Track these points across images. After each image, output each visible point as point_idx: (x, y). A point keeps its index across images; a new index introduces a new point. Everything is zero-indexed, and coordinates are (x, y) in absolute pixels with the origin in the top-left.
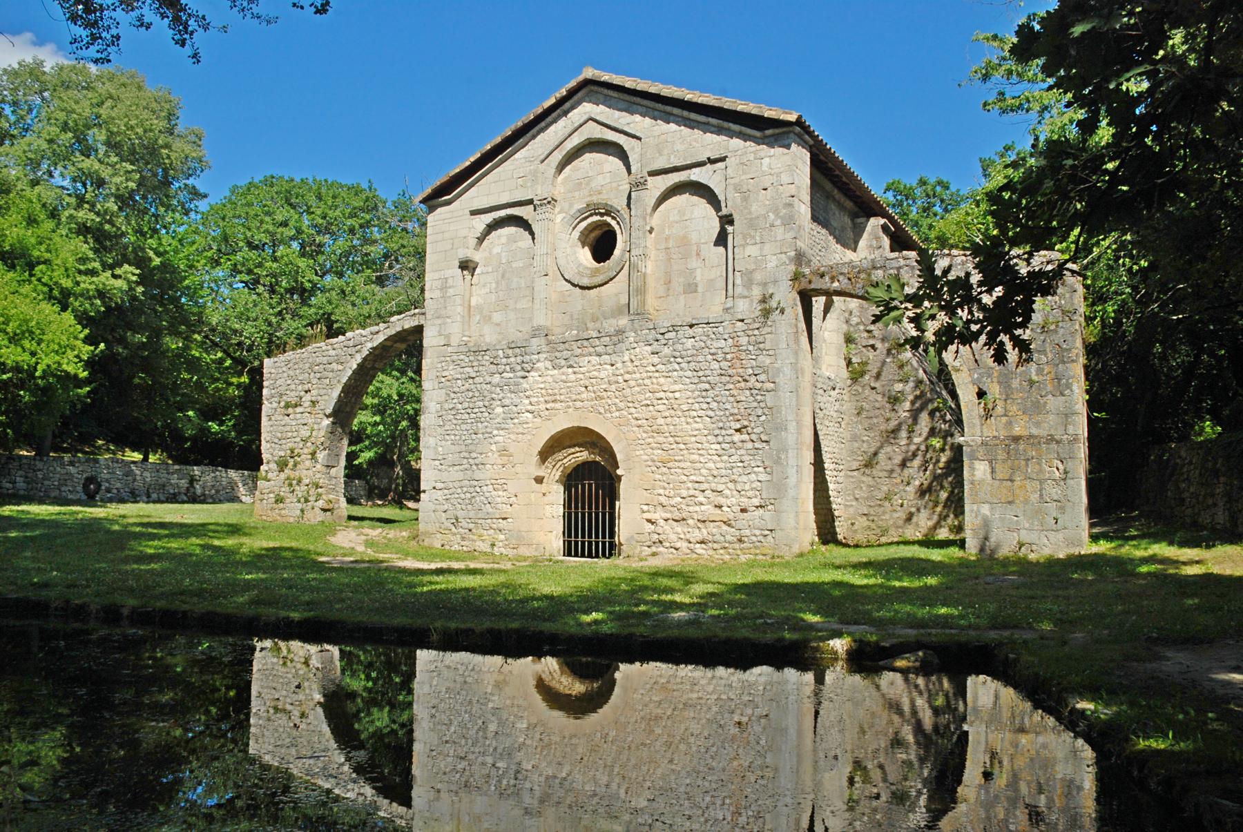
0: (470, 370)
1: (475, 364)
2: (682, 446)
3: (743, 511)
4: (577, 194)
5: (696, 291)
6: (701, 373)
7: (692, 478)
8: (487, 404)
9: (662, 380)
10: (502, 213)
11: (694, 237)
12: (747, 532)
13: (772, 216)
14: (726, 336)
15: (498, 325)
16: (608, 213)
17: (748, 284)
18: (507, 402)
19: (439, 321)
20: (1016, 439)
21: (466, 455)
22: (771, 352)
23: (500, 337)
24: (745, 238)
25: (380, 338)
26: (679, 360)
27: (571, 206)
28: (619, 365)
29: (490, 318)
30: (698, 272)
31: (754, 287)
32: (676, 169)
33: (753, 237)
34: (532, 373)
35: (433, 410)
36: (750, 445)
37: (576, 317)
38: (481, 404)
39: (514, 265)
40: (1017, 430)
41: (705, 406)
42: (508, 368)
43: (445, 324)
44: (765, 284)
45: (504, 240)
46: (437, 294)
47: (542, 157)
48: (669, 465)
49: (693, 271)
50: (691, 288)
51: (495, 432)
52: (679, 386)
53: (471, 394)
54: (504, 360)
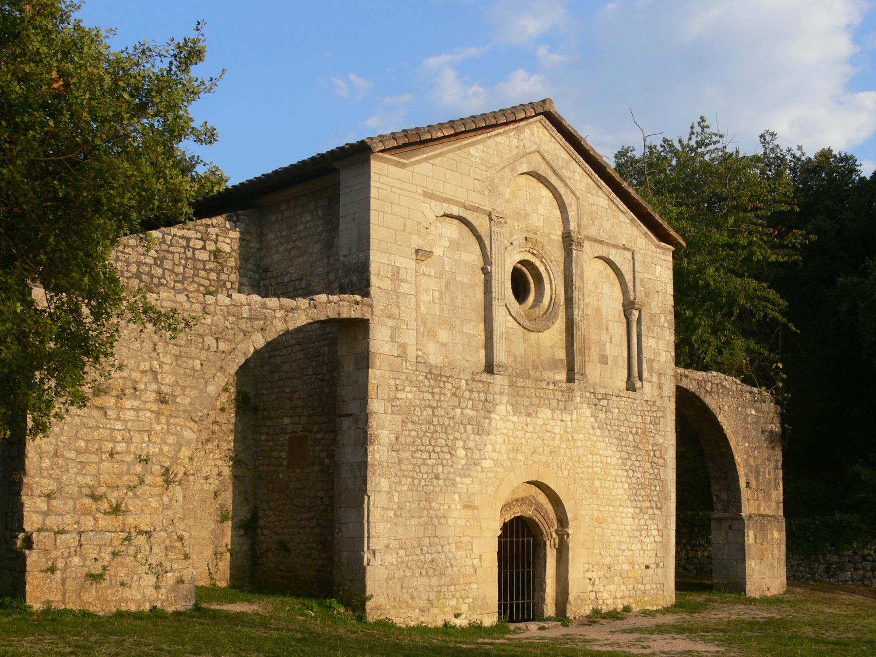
0: (429, 396)
1: (437, 390)
2: (611, 509)
3: (647, 567)
4: (516, 224)
5: (607, 364)
6: (623, 443)
7: (617, 538)
8: (450, 443)
9: (598, 444)
10: (455, 211)
11: (604, 311)
12: (648, 587)
13: (663, 319)
14: (638, 413)
15: (444, 345)
16: (541, 258)
17: (651, 370)
18: (471, 444)
19: (391, 323)
20: (763, 516)
21: (428, 504)
22: (663, 433)
23: (446, 361)
24: (648, 328)
25: (300, 320)
26: (609, 427)
27: (511, 234)
28: (569, 423)
29: (435, 336)
30: (608, 345)
31: (654, 374)
32: (601, 242)
33: (653, 331)
34: (493, 415)
35: (386, 441)
36: (650, 511)
37: (519, 360)
38: (443, 443)
39: (458, 278)
40: (762, 511)
41: (625, 474)
42: (470, 402)
43: (399, 328)
44: (660, 374)
45: (446, 243)
46: (387, 284)
47: (498, 168)
48: (604, 525)
49: (604, 345)
50: (603, 360)
51: (458, 479)
52: (608, 453)
53: (432, 428)
54: (467, 394)
